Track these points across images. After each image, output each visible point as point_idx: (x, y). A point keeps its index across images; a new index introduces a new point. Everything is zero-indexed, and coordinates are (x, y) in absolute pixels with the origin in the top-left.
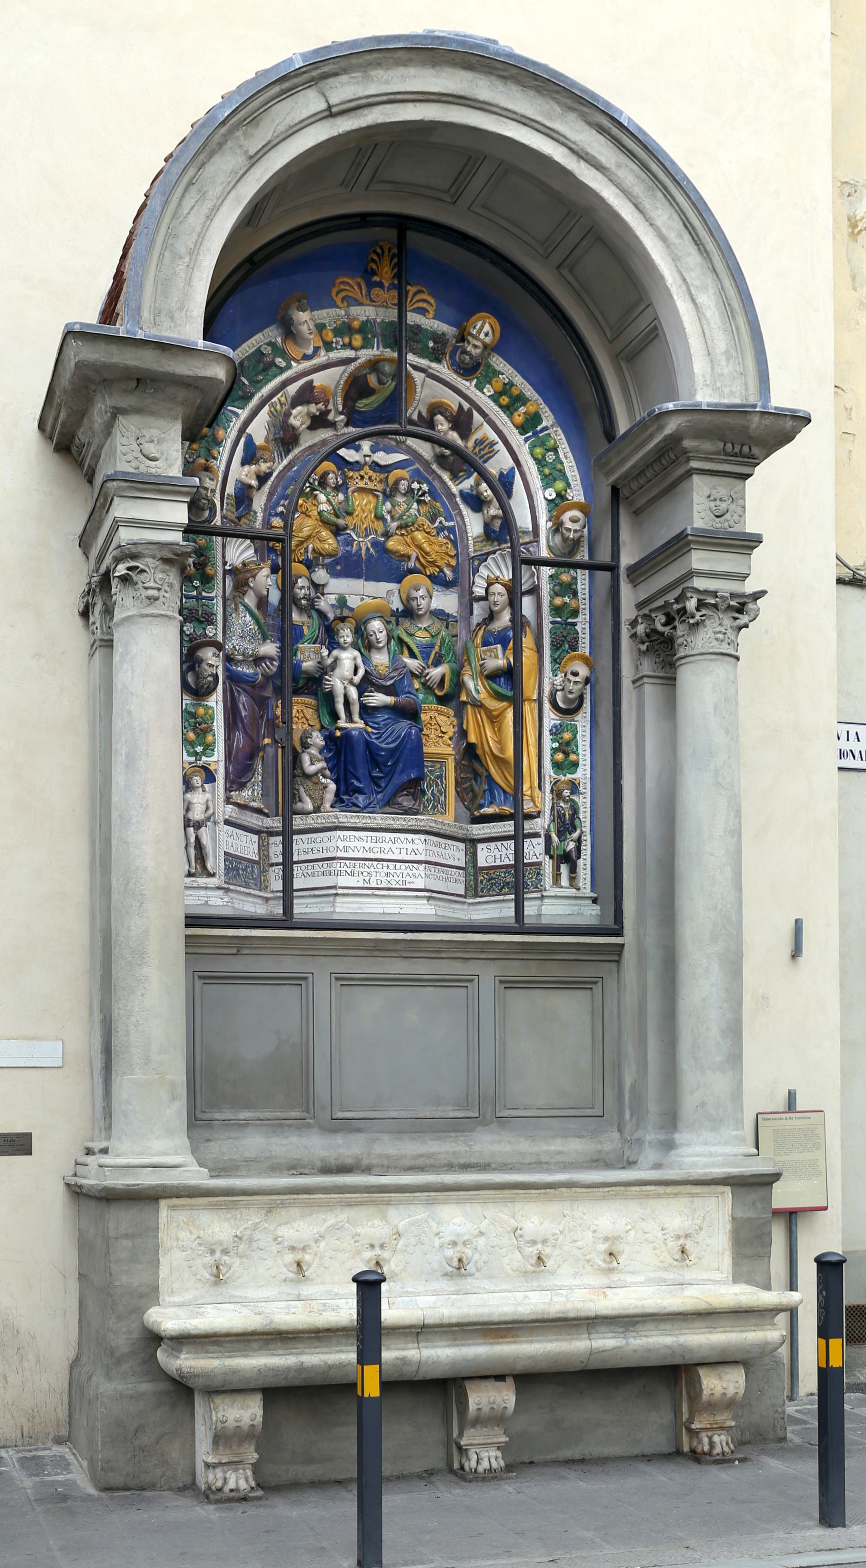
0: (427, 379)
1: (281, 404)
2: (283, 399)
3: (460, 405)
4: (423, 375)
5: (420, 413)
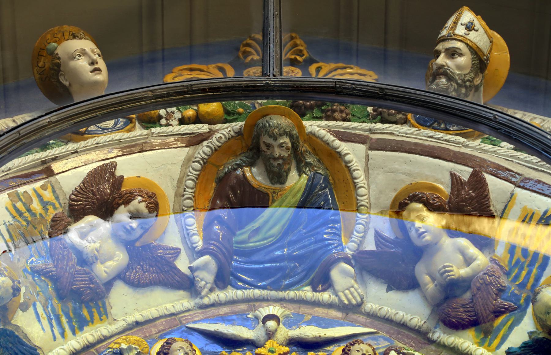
0: (372, 153)
1: (45, 204)
2: (48, 195)
3: (453, 176)
4: (361, 148)
5: (378, 236)
